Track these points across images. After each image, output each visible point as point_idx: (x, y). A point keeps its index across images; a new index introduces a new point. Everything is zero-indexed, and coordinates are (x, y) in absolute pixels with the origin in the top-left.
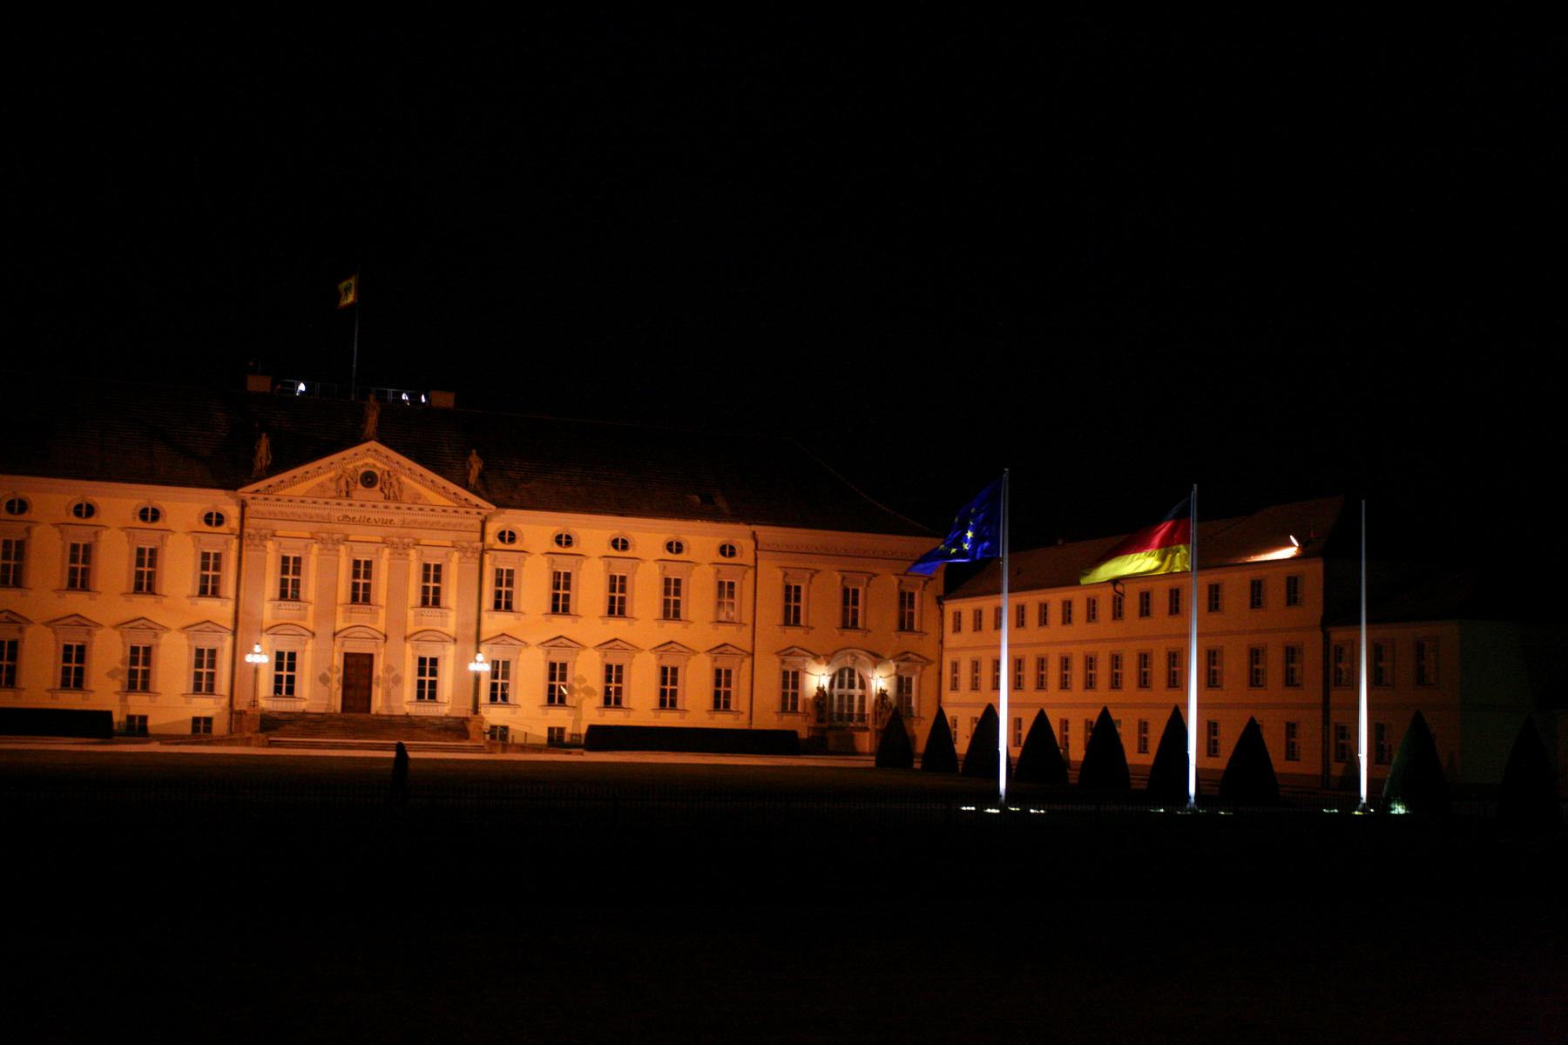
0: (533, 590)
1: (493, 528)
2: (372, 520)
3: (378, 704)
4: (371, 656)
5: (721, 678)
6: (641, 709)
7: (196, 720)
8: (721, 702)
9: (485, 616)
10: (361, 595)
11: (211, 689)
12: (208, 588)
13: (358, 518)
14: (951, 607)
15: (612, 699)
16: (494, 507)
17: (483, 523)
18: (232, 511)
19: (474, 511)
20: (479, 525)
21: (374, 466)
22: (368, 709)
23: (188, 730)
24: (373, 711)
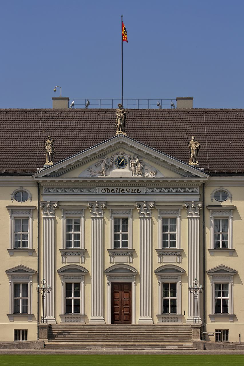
1: (209, 192)
2: (125, 190)
4: (130, 284)
7: (17, 332)
9: (208, 254)
11: (25, 310)
13: (115, 190)
16: (208, 176)
17: (203, 186)
18: (33, 191)
19: (194, 180)
20: (198, 190)
21: (124, 153)
23: (10, 337)
24: (133, 323)
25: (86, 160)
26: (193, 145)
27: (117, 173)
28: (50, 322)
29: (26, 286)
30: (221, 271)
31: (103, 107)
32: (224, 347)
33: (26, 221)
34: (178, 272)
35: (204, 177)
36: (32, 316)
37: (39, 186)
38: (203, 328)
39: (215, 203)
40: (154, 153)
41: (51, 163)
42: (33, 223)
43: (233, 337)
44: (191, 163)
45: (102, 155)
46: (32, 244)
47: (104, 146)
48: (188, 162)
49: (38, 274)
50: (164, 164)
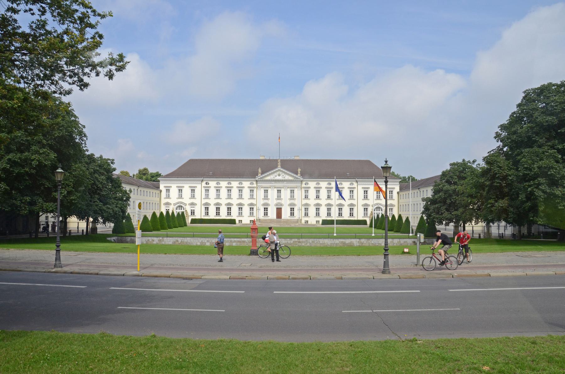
0: (312, 193)
1: (304, 183)
3: (283, 217)
4: (281, 208)
5: (351, 209)
6: (335, 216)
8: (351, 214)
10: (279, 197)
11: (253, 215)
12: (252, 197)
14: (400, 193)
15: (329, 214)
17: (302, 181)
18: (255, 183)
22: (281, 218)
25: (270, 174)
26: (299, 170)
27: (278, 178)
28: (260, 218)
29: (253, 208)
30: (307, 205)
31: (274, 159)
32: (307, 225)
33: (253, 191)
34: (294, 205)
35: (302, 179)
36: (255, 216)
37: (257, 181)
38: (301, 220)
39: (305, 186)
40: (288, 172)
41: (260, 175)
42: (255, 191)
43: (309, 223)
44: (299, 175)
45: (274, 172)
46: (255, 197)
47: (275, 171)
48: (297, 175)
49: (256, 205)
50: (291, 176)
